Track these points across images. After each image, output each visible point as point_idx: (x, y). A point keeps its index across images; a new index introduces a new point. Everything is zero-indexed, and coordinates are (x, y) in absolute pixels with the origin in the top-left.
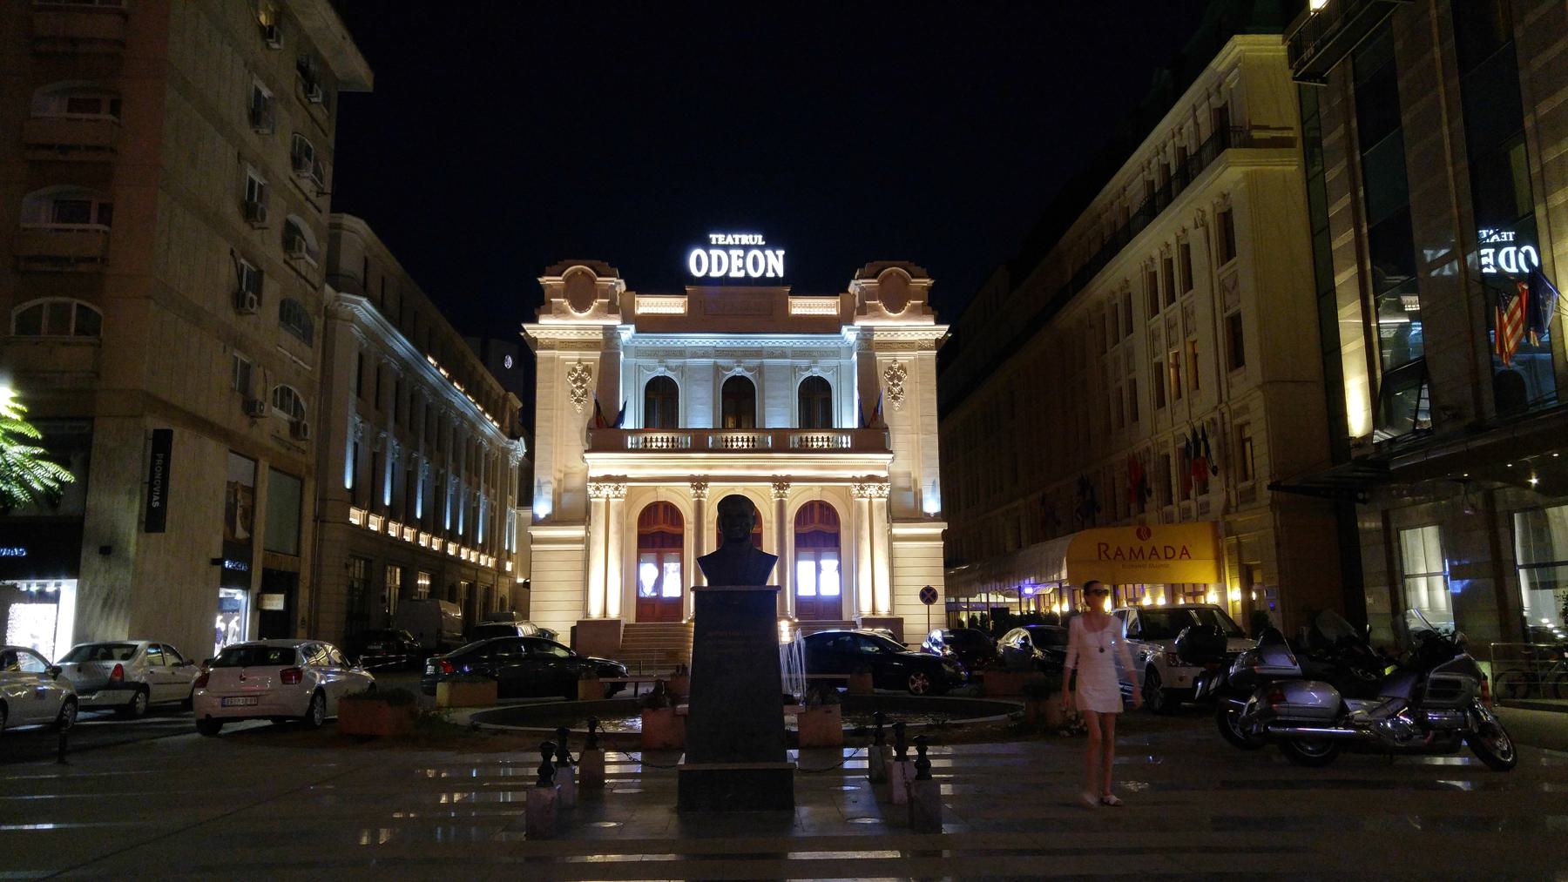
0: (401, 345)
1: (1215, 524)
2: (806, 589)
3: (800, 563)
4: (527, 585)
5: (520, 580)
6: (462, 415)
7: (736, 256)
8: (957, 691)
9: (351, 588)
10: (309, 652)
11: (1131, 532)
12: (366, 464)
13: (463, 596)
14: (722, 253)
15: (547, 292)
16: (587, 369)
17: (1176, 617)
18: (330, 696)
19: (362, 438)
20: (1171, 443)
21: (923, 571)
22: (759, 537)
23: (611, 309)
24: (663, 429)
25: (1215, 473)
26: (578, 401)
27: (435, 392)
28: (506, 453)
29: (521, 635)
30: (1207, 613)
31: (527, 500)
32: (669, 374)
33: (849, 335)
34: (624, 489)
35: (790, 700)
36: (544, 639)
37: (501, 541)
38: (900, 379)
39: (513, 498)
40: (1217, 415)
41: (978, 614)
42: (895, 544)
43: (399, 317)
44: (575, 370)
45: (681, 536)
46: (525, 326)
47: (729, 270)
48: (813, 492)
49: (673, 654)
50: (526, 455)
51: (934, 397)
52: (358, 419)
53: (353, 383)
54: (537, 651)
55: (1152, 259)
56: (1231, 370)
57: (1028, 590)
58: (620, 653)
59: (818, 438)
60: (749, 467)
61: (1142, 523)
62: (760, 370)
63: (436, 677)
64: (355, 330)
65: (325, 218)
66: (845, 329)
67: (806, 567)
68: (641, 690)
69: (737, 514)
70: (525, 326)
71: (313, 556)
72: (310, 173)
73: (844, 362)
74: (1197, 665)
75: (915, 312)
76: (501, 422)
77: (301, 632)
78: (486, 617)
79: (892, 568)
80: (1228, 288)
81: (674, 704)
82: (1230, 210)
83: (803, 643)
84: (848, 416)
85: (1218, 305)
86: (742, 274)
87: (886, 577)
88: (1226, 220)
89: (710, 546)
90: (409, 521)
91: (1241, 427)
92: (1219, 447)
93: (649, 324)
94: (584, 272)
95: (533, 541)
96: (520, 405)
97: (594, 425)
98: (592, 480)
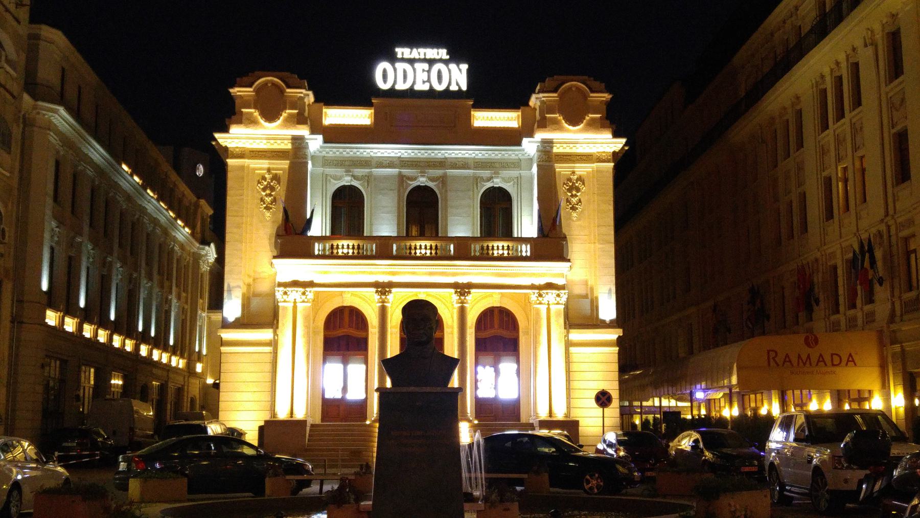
0: (97, 152)
1: (880, 333)
2: (486, 392)
4: (216, 386)
5: (210, 381)
6: (155, 222)
7: (420, 69)
8: (629, 490)
10: (6, 448)
11: (800, 339)
12: (61, 264)
13: (154, 396)
15: (237, 102)
16: (276, 178)
18: (26, 490)
19: (58, 243)
20: (839, 252)
21: (599, 376)
22: (441, 341)
23: (300, 120)
24: (349, 236)
25: (881, 284)
26: (267, 208)
27: (129, 198)
28: (197, 258)
29: (210, 432)
30: (872, 418)
31: (217, 303)
32: (356, 183)
33: (530, 146)
34: (311, 292)
35: (470, 498)
36: (233, 438)
37: (192, 343)
38: (578, 190)
39: (204, 302)
40: (883, 227)
41: (650, 417)
42: (572, 349)
43: (95, 126)
44: (264, 178)
46: (217, 135)
47: (414, 83)
48: (493, 299)
49: (357, 454)
51: (611, 208)
52: (54, 224)
53: (50, 187)
54: (225, 450)
55: (822, 77)
56: (897, 184)
57: (700, 395)
58: (303, 451)
59: (499, 246)
60: (431, 274)
61: (810, 331)
62: (443, 180)
64: (53, 138)
65: (24, 29)
66: (525, 141)
67: (485, 373)
68: (327, 488)
69: (420, 319)
70: (217, 135)
73: (524, 173)
74: (862, 467)
75: (594, 126)
76: (193, 228)
79: (568, 372)
80: (897, 105)
81: (358, 500)
82: (899, 29)
83: (482, 442)
84: (527, 224)
85: (885, 122)
86: (426, 87)
87: (565, 381)
88: (894, 39)
89: (393, 349)
90: (103, 322)
91: (906, 240)
92: (884, 258)
93: (335, 135)
94: (274, 84)
95: (223, 343)
96: (211, 212)
97: (282, 232)
98: (280, 285)
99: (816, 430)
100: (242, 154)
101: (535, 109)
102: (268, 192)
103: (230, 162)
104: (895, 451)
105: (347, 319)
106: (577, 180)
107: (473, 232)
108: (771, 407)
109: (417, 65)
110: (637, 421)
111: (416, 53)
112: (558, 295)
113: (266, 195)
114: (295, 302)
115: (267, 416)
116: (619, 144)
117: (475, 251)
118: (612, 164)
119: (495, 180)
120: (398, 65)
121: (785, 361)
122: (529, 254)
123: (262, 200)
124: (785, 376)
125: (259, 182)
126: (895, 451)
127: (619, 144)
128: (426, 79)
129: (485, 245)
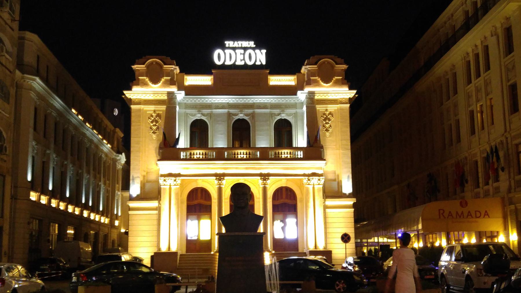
0: (58, 102)
1: (503, 199)
2: (279, 235)
3: (275, 222)
4: (126, 233)
5: (123, 230)
6: (91, 141)
7: (240, 53)
9: (31, 235)
10: (9, 270)
11: (457, 202)
13: (92, 239)
14: (232, 52)
15: (137, 73)
16: (158, 115)
17: (481, 250)
19: (37, 154)
20: (479, 154)
21: (342, 225)
22: (253, 206)
23: (172, 82)
26: (154, 133)
27: (76, 128)
28: (115, 161)
29: (123, 260)
30: (499, 247)
31: (126, 187)
32: (203, 118)
33: (302, 96)
34: (179, 180)
36: (136, 262)
38: (329, 120)
39: (119, 186)
40: (503, 139)
41: (373, 248)
43: (56, 87)
44: (152, 116)
45: (210, 206)
46: (125, 92)
47: (236, 61)
48: (282, 182)
49: (206, 271)
50: (126, 162)
52: (34, 143)
55: (468, 54)
59: (285, 152)
60: (247, 168)
61: (463, 198)
62: (253, 116)
63: (78, 283)
64: (33, 95)
66: (299, 92)
67: (278, 224)
68: (189, 290)
69: (241, 194)
70: (125, 92)
71: (10, 218)
72: (8, 9)
73: (298, 110)
74: (493, 275)
75: (338, 83)
76: (112, 144)
77: (4, 259)
78: (104, 251)
79: (325, 223)
80: (510, 69)
83: (277, 264)
84: (301, 139)
86: (242, 63)
87: (325, 228)
88: (508, 32)
89: (226, 211)
90: (62, 198)
91: (517, 145)
92: (505, 156)
93: (192, 91)
95: (130, 209)
97: (163, 146)
98: (162, 176)
99: (467, 254)
100: (139, 103)
101: (304, 75)
102: (154, 123)
103: (133, 107)
104: (512, 266)
105: (199, 195)
106: (329, 114)
107: (270, 145)
108: (442, 242)
109: (237, 51)
110: (365, 251)
111: (237, 44)
112: (319, 180)
113: (153, 125)
114: (170, 186)
115: (155, 250)
116: (352, 93)
117: (271, 155)
118: (348, 105)
119: (283, 115)
120: (226, 51)
121: (449, 215)
122: (302, 157)
123: (151, 128)
124: (449, 224)
125: (149, 118)
126: (512, 266)
127: (352, 93)
128: (242, 58)
129: (277, 152)
